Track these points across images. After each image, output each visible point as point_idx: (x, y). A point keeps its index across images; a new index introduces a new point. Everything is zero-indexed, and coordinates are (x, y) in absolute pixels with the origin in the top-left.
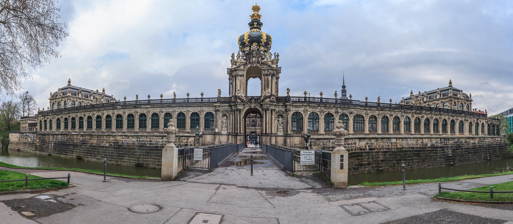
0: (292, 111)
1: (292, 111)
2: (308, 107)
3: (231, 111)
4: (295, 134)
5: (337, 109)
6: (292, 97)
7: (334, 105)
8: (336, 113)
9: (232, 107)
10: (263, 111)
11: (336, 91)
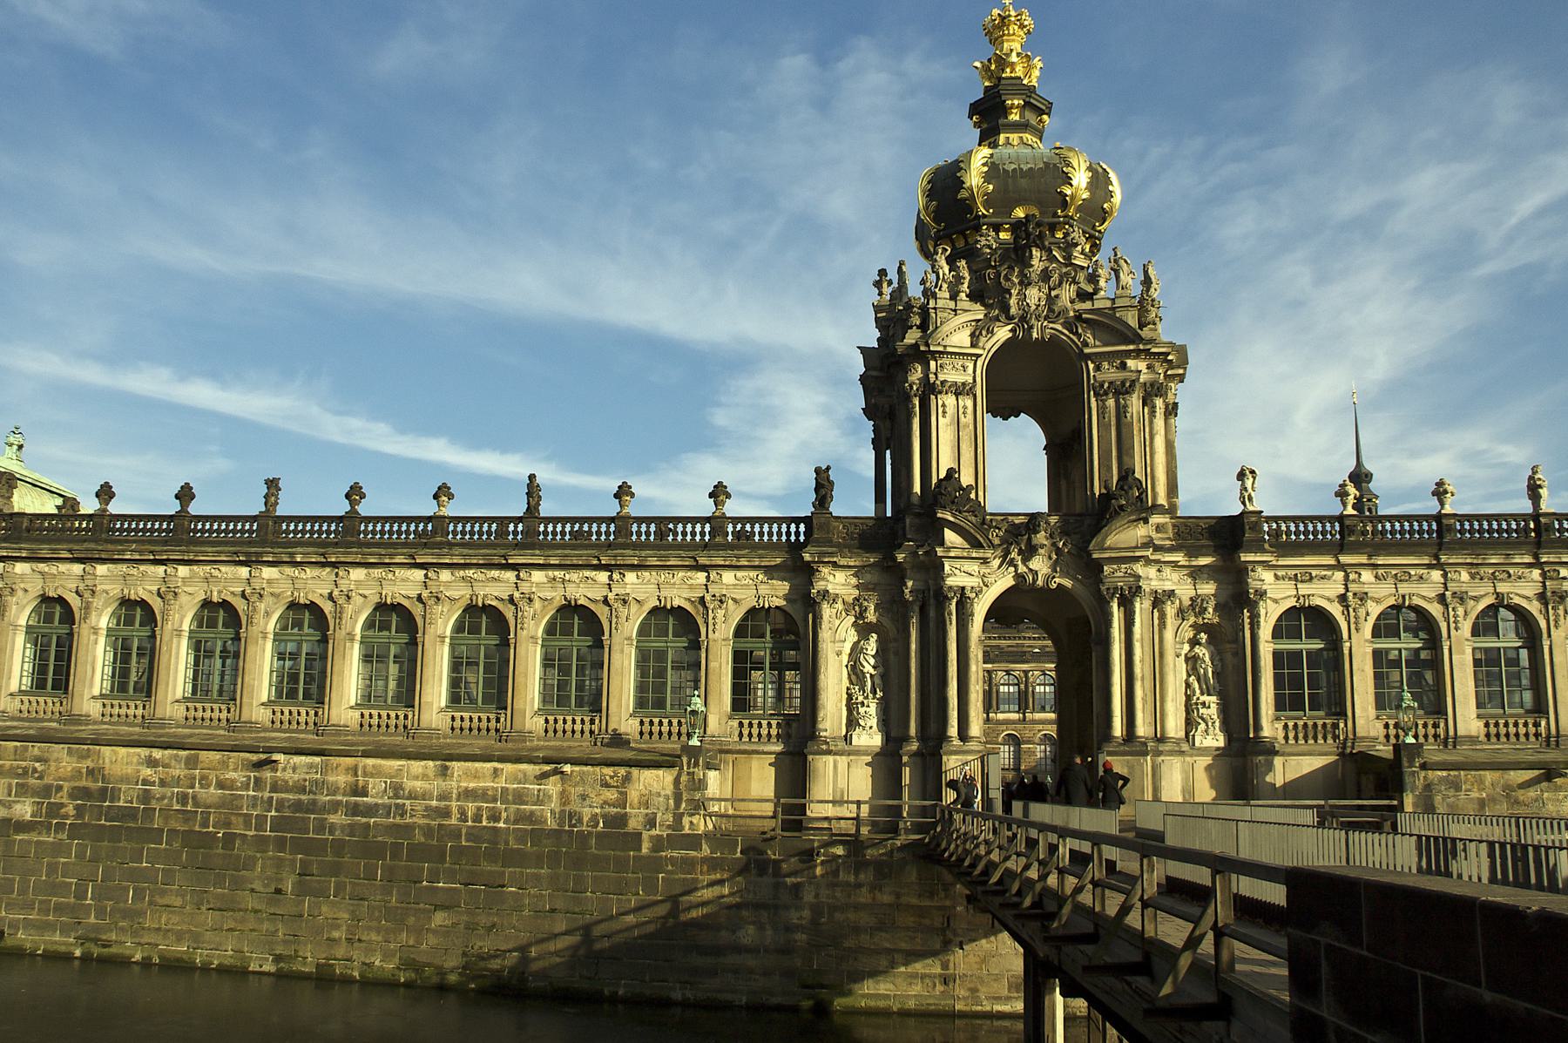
0: (1276, 601)
1: (1276, 601)
2: (1367, 576)
4: (1296, 738)
6: (1269, 519)
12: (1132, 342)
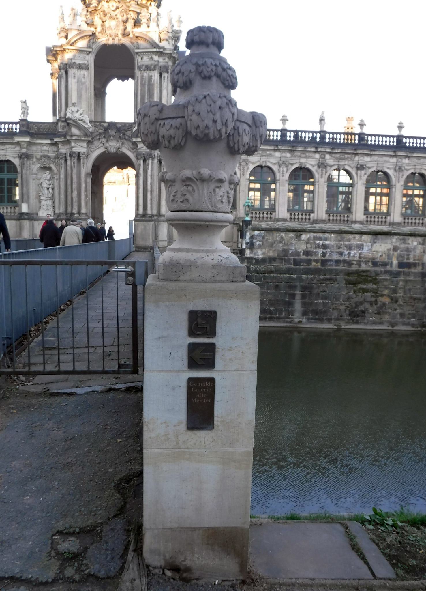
3: (57, 157)
5: (324, 158)
7: (316, 148)
8: (319, 167)
9: (60, 146)
10: (137, 159)
11: (323, 113)
12: (155, 48)
